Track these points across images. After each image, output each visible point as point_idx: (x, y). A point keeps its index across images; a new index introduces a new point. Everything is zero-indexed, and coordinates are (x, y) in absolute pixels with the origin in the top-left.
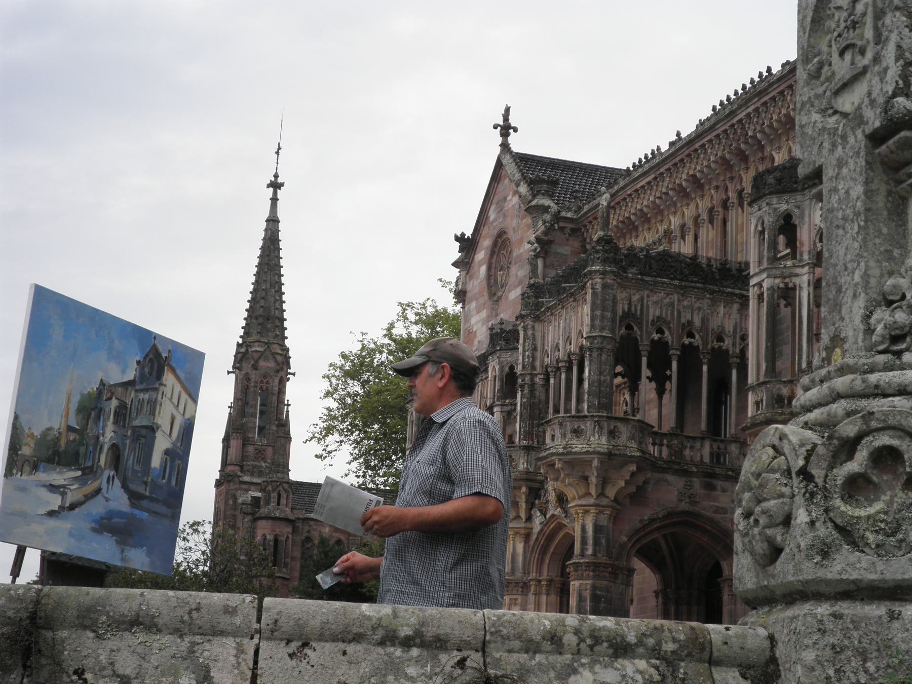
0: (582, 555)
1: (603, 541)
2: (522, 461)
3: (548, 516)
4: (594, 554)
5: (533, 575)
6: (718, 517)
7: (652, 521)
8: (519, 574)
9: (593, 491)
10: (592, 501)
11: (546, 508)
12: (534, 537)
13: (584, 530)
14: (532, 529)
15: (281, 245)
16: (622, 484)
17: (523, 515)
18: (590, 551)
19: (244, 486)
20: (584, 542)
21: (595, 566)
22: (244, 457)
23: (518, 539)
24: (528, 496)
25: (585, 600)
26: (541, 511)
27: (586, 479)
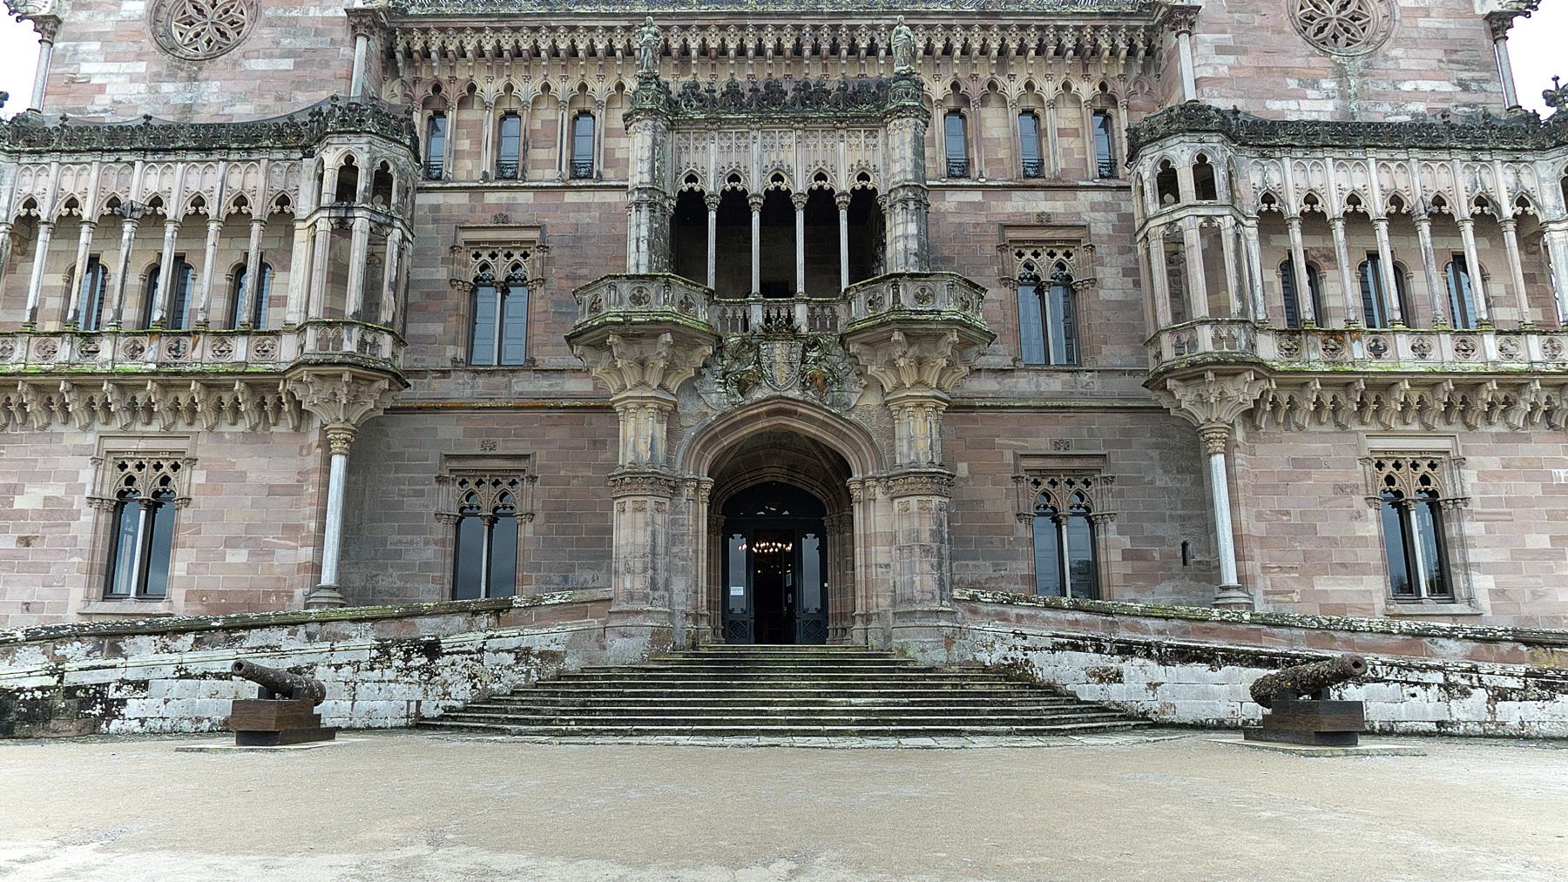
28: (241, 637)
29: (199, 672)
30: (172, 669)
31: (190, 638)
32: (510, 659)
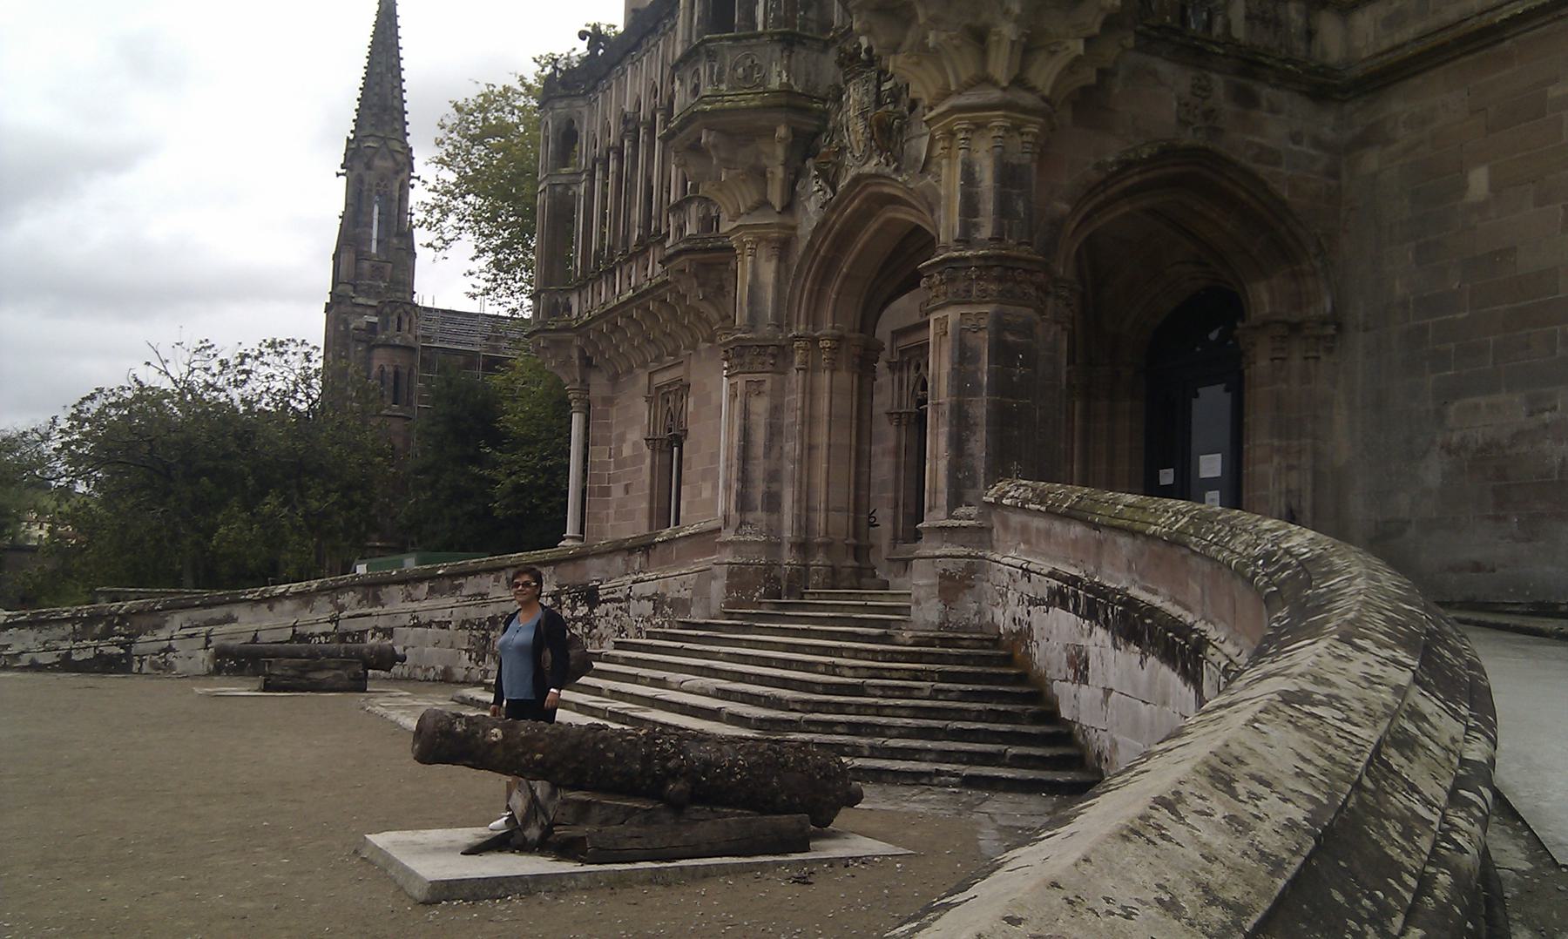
0: (965, 240)
1: (1020, 207)
2: (775, 69)
3: (842, 184)
4: (997, 238)
5: (800, 329)
6: (1263, 170)
7: (1126, 165)
8: (765, 330)
9: (1000, 66)
10: (995, 95)
11: (839, 166)
12: (801, 246)
13: (969, 176)
14: (794, 228)
15: (399, 22)
16: (1078, 47)
17: (775, 196)
18: (986, 232)
19: (358, 310)
20: (970, 207)
21: (999, 267)
22: (358, 275)
23: (762, 253)
24: (791, 148)
25: (976, 359)
26: (823, 174)
27: (979, 37)
28: (461, 585)
29: (426, 620)
30: (408, 617)
31: (425, 586)
32: (648, 607)
